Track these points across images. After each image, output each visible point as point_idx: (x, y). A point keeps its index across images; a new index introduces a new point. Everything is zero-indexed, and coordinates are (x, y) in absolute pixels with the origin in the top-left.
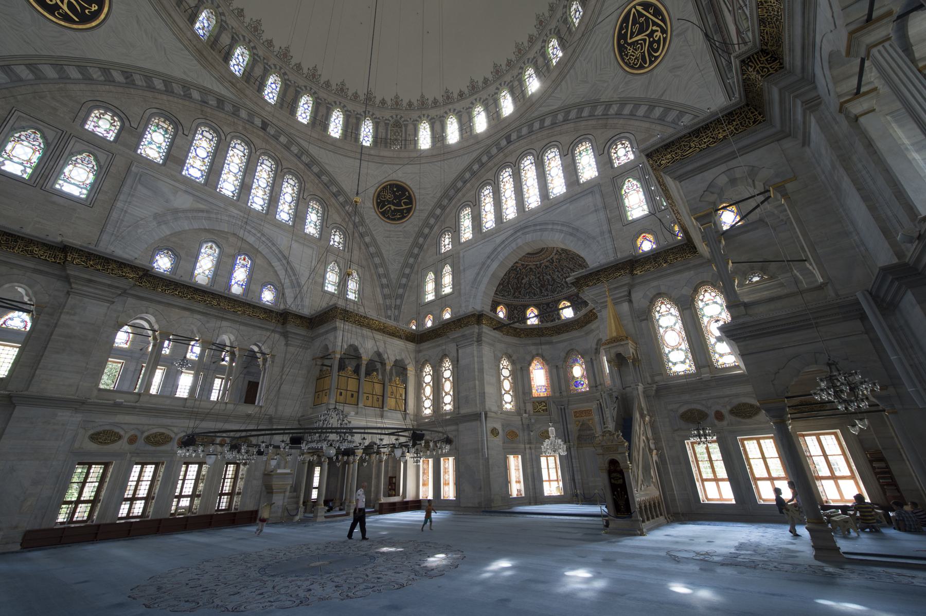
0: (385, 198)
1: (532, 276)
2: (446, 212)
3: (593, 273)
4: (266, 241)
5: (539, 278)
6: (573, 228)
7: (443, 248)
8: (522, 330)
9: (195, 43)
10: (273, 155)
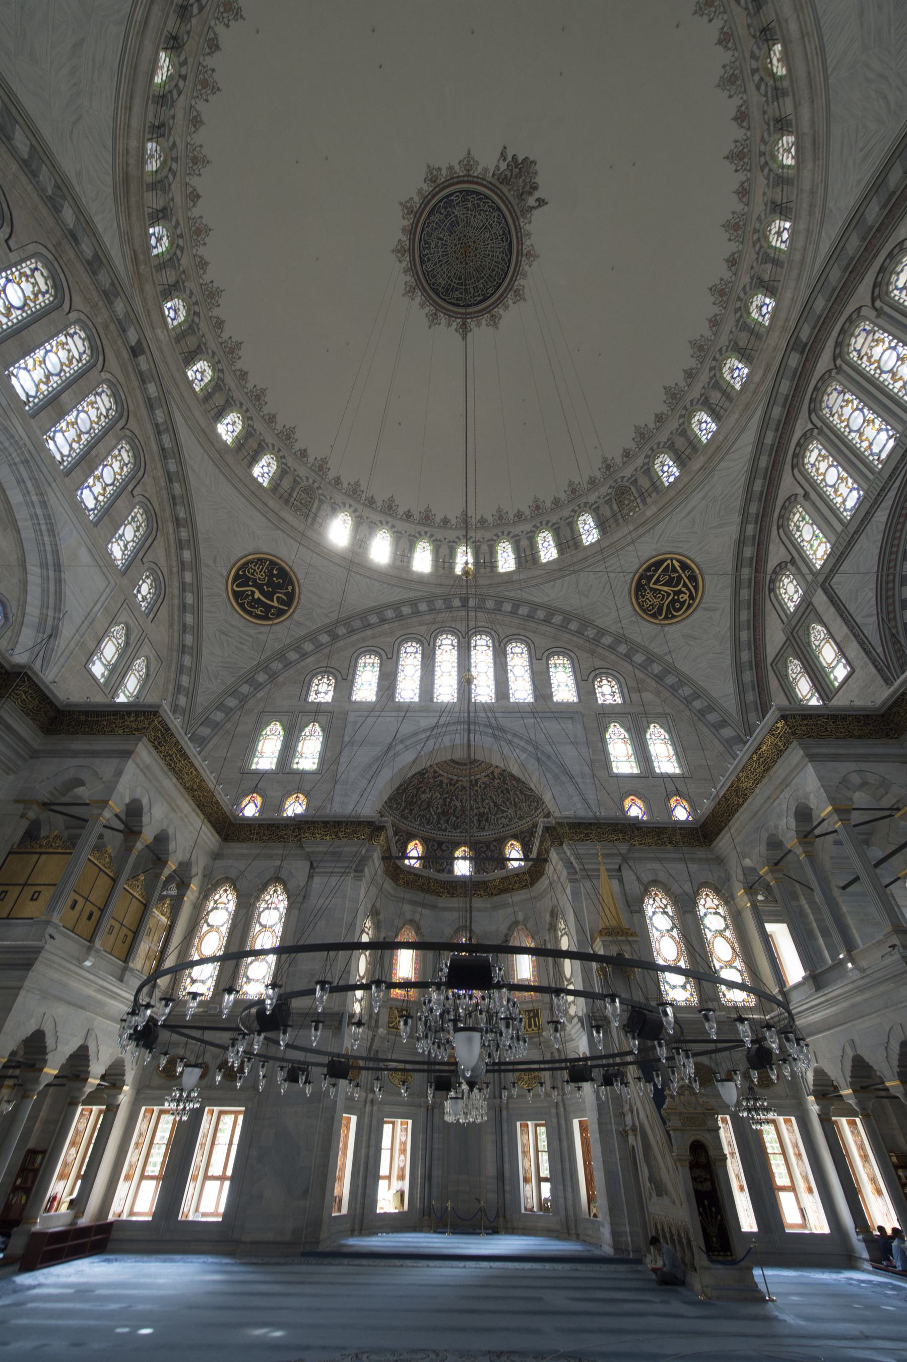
0: (252, 574)
4: (41, 517)
6: (543, 752)
9: (132, 161)
10: (123, 397)
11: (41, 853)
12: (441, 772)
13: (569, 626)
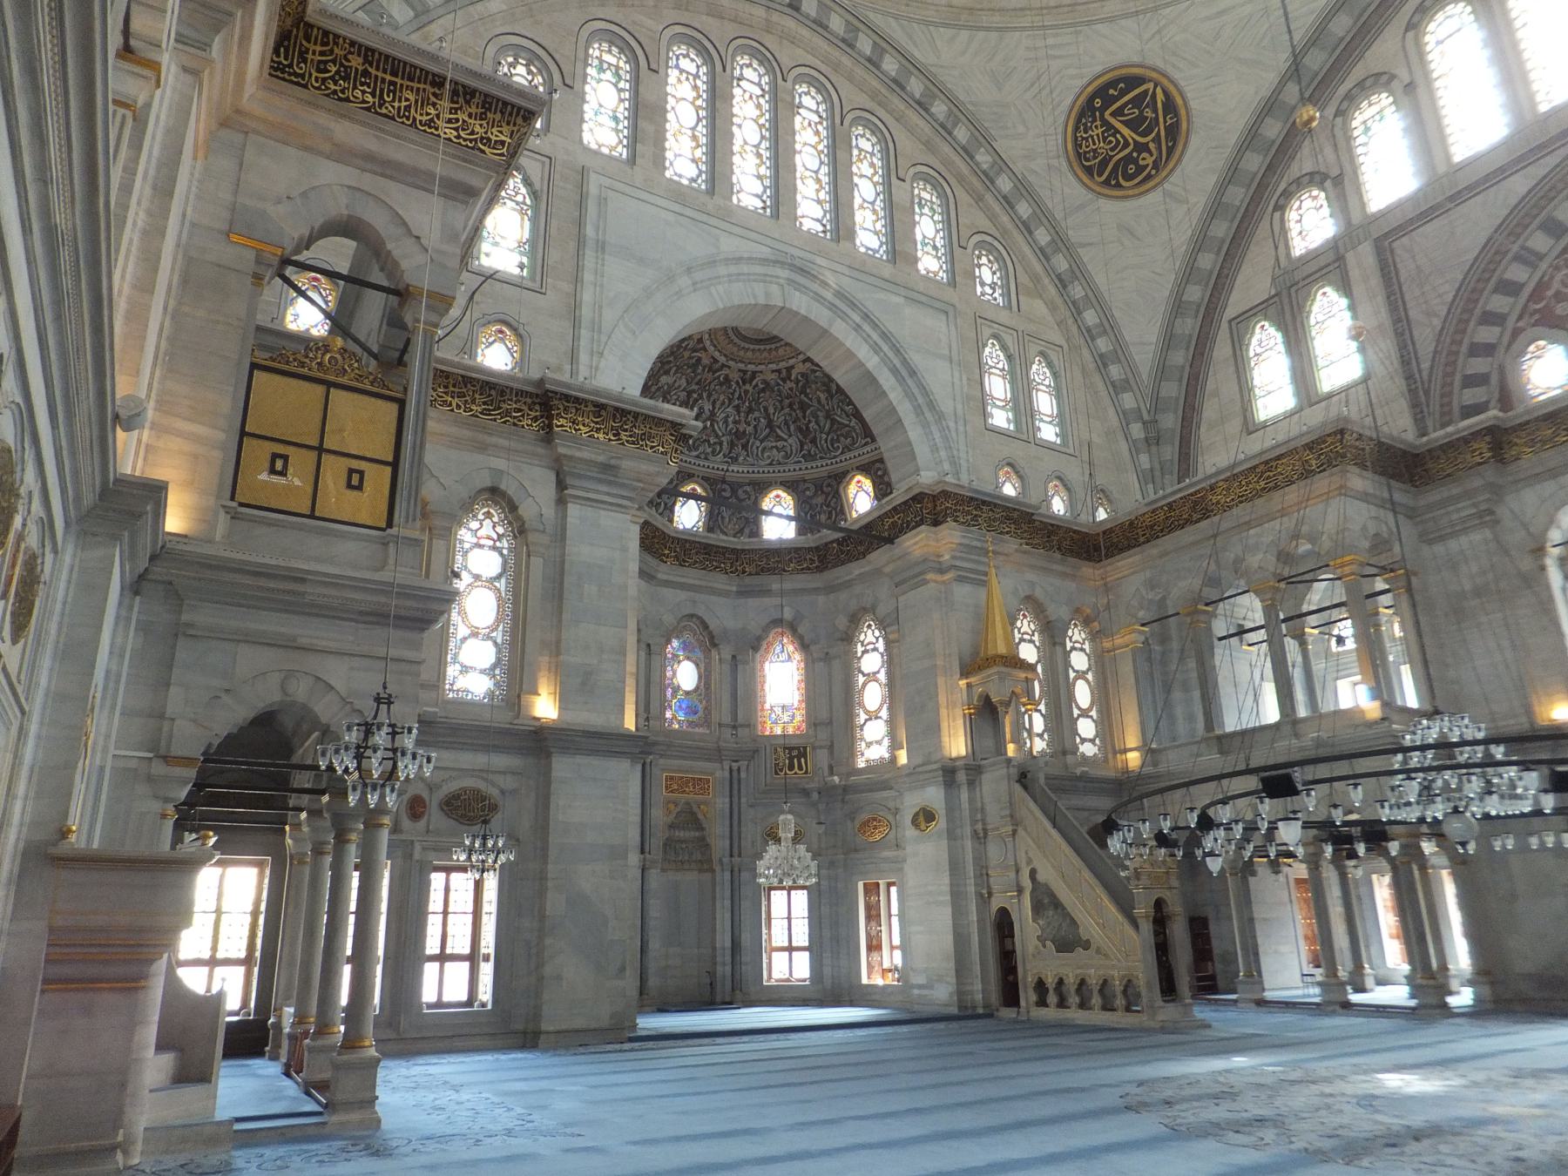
1: (683, 382)
11: (330, 385)
13: (955, 133)
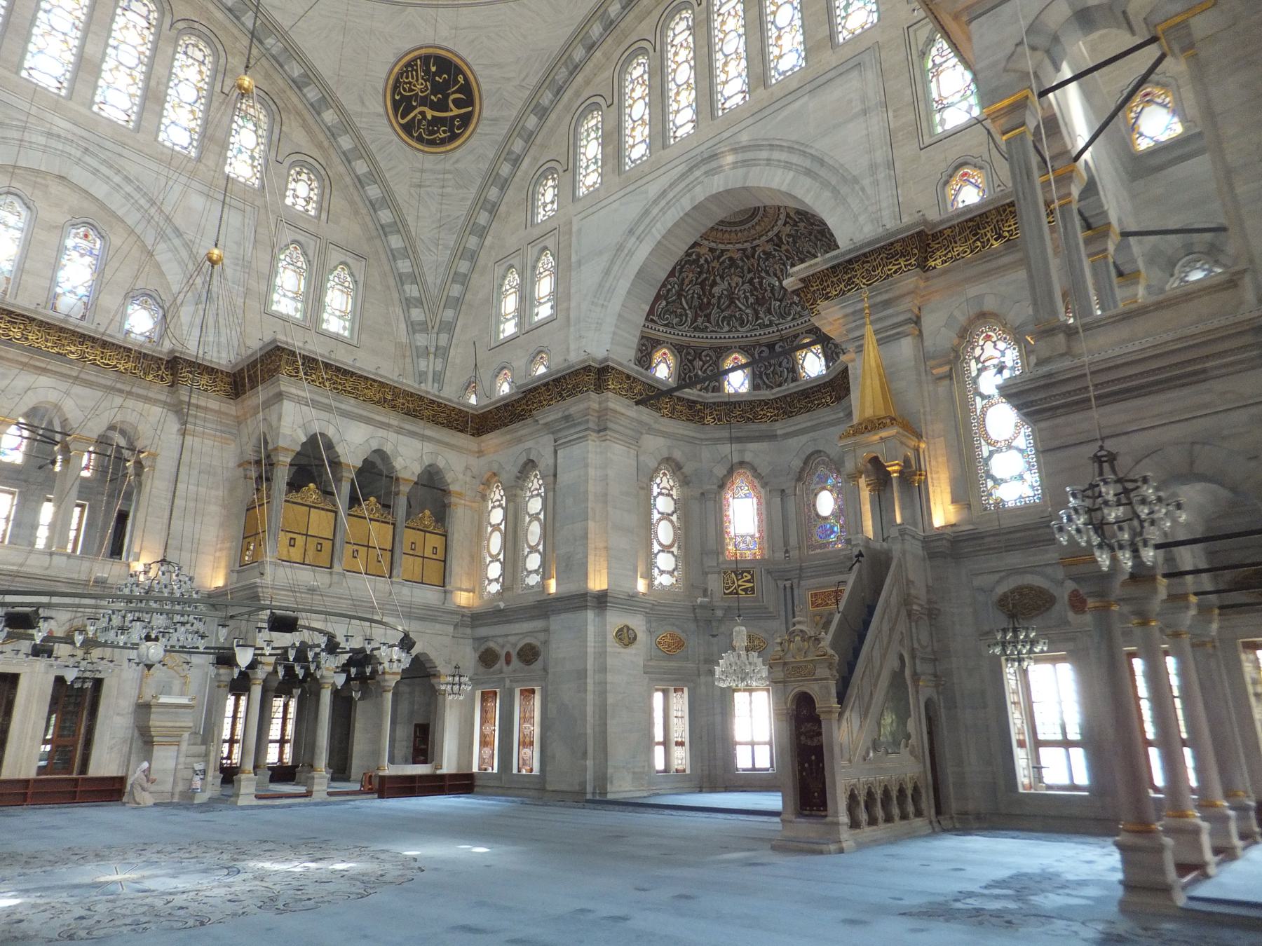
1: (736, 279)
2: (549, 123)
3: (839, 265)
5: (751, 282)
7: (541, 210)
8: (706, 405)
12: (721, 246)
